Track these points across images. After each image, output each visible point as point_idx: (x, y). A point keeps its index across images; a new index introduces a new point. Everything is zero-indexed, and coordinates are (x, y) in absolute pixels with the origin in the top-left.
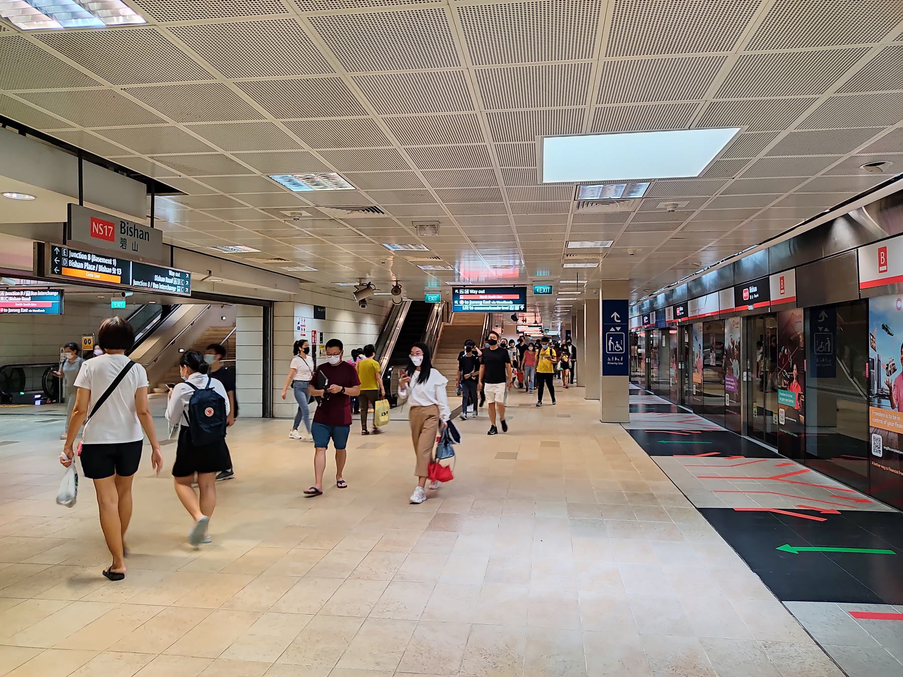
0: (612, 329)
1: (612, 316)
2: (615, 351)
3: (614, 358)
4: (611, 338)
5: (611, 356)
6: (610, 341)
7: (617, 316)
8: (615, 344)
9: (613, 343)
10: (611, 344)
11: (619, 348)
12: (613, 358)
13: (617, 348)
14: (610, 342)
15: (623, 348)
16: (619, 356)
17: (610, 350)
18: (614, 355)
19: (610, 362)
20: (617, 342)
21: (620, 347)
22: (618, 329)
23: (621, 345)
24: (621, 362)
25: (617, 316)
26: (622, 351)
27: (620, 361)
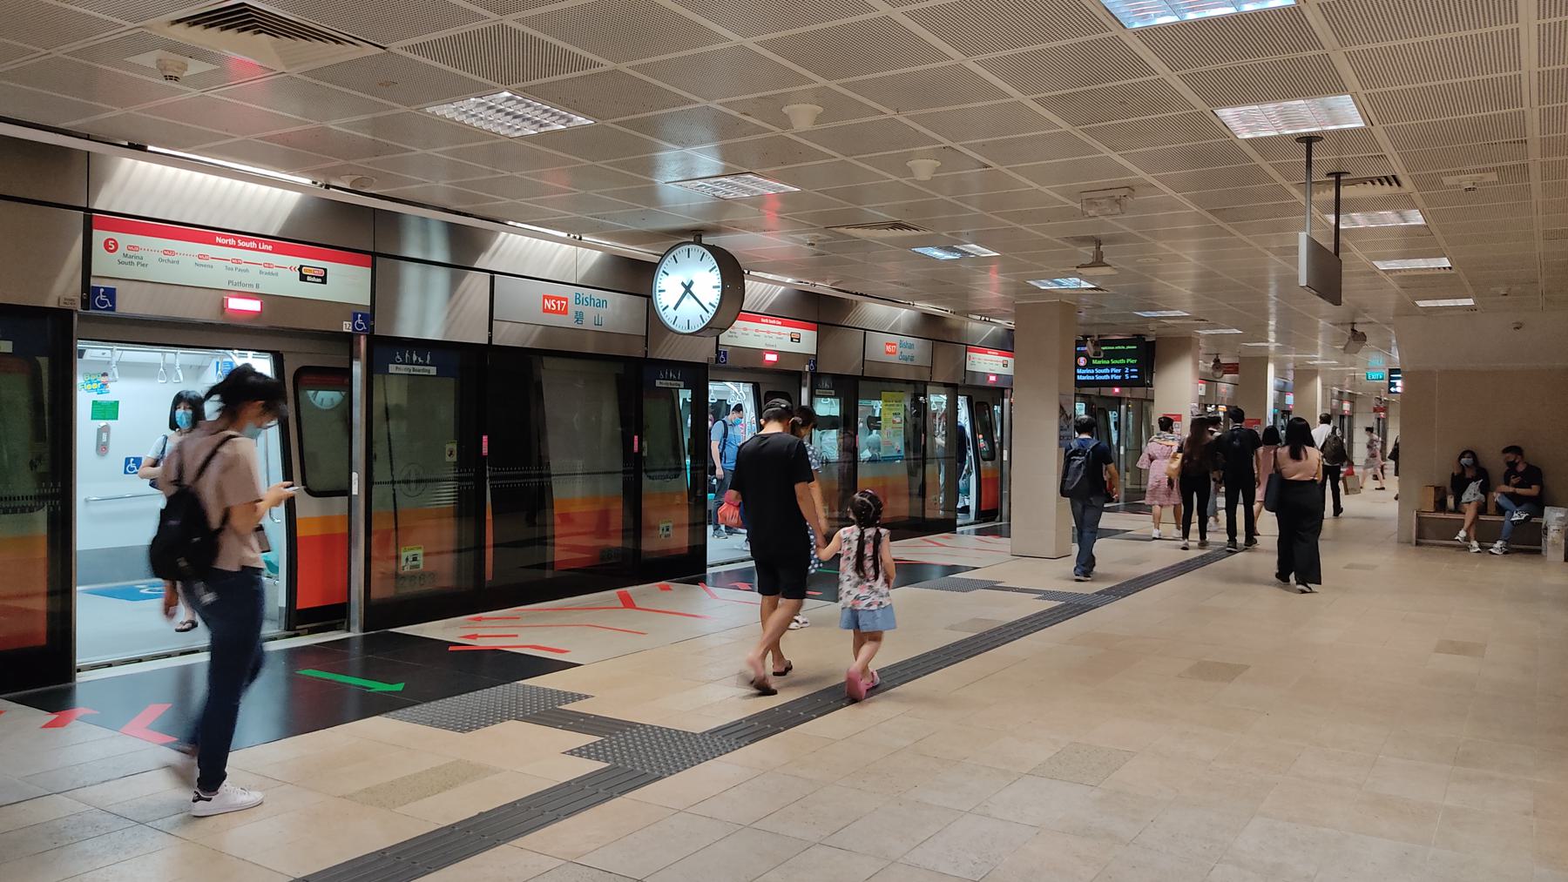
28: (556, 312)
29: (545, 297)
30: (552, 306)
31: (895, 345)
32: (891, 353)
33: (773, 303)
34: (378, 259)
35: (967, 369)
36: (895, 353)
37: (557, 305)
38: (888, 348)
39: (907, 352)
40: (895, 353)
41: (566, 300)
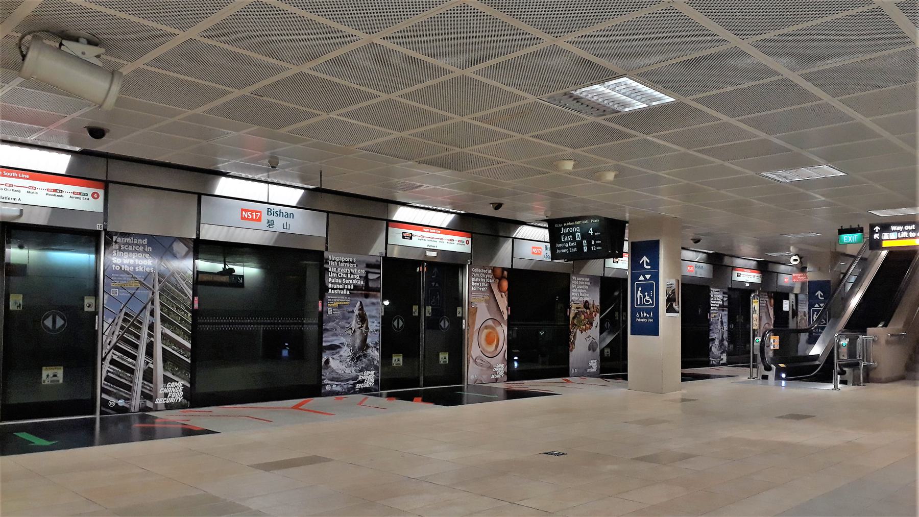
3: (644, 314)
4: (640, 289)
5: (639, 311)
6: (639, 292)
7: (646, 261)
8: (645, 296)
9: (642, 295)
10: (640, 295)
11: (648, 301)
17: (639, 303)
18: (643, 310)
19: (638, 318)
20: (646, 294)
21: (650, 300)
22: (648, 277)
24: (651, 318)
25: (646, 261)
26: (652, 305)
27: (650, 318)
28: (252, 219)
29: (242, 210)
30: (248, 216)
34: (111, 185)
37: (252, 216)
41: (260, 212)
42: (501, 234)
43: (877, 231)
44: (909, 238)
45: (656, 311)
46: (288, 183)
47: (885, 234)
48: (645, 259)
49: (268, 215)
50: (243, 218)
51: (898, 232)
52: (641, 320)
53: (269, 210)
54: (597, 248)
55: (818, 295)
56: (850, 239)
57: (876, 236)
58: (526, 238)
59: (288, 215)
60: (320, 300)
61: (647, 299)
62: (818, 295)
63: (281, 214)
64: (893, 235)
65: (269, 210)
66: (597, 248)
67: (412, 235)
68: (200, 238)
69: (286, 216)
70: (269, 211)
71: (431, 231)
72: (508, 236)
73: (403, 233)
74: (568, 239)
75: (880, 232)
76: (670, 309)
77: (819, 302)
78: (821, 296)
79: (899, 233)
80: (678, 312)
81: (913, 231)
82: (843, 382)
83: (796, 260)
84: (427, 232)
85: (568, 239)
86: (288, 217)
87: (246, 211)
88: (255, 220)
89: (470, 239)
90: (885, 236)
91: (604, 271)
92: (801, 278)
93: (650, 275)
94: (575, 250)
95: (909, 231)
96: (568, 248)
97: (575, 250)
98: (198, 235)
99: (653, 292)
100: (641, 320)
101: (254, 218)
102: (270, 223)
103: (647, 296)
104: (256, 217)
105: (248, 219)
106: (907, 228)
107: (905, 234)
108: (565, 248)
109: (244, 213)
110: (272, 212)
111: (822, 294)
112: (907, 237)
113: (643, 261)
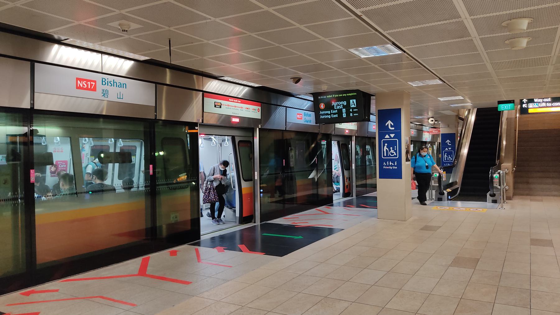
0: (387, 136)
1: (386, 124)
2: (390, 156)
3: (389, 163)
4: (386, 144)
5: (386, 161)
6: (385, 147)
8: (390, 150)
9: (388, 149)
10: (386, 150)
11: (393, 153)
12: (388, 163)
13: (391, 152)
14: (385, 148)
15: (397, 153)
16: (393, 160)
18: (389, 160)
19: (385, 166)
20: (391, 148)
21: (394, 152)
22: (392, 135)
23: (395, 151)
28: (87, 89)
29: (77, 79)
31: (302, 115)
32: (300, 119)
33: (195, 83)
35: (336, 127)
36: (302, 119)
37: (87, 85)
38: (298, 116)
39: (308, 118)
40: (302, 119)
41: (95, 82)
42: (273, 103)
43: (525, 102)
44: (547, 107)
45: (399, 161)
46: (121, 53)
47: (530, 104)
48: (389, 123)
49: (102, 84)
50: (78, 88)
51: (539, 103)
52: (387, 168)
53: (104, 80)
54: (354, 115)
55: (447, 142)
56: (506, 108)
57: (524, 106)
58: (290, 106)
59: (121, 85)
60: (151, 164)
61: (392, 152)
62: (447, 142)
63: (115, 83)
64: (535, 105)
65: (104, 80)
66: (354, 115)
67: (221, 105)
68: (35, 108)
69: (120, 86)
70: (103, 82)
71: (235, 101)
72: (279, 104)
73: (215, 102)
74: (339, 107)
75: (527, 103)
76: (407, 160)
77: (448, 147)
78: (449, 143)
79: (540, 104)
80: (410, 161)
81: (549, 102)
82: (495, 202)
83: (432, 121)
84: (231, 101)
85: (339, 107)
86: (121, 87)
87: (81, 80)
88: (90, 89)
89: (260, 108)
90: (531, 105)
91: (286, 125)
92: (435, 132)
93: (394, 134)
94: (336, 116)
95: (547, 102)
96: (331, 114)
97: (336, 116)
98: (33, 104)
99: (397, 147)
100: (387, 168)
101: (89, 87)
102: (105, 93)
103: (391, 150)
104: (91, 87)
105: (83, 89)
106: (545, 100)
107: (544, 104)
108: (327, 114)
109: (79, 82)
110: (106, 82)
111: (450, 142)
112: (545, 106)
113: (388, 124)
